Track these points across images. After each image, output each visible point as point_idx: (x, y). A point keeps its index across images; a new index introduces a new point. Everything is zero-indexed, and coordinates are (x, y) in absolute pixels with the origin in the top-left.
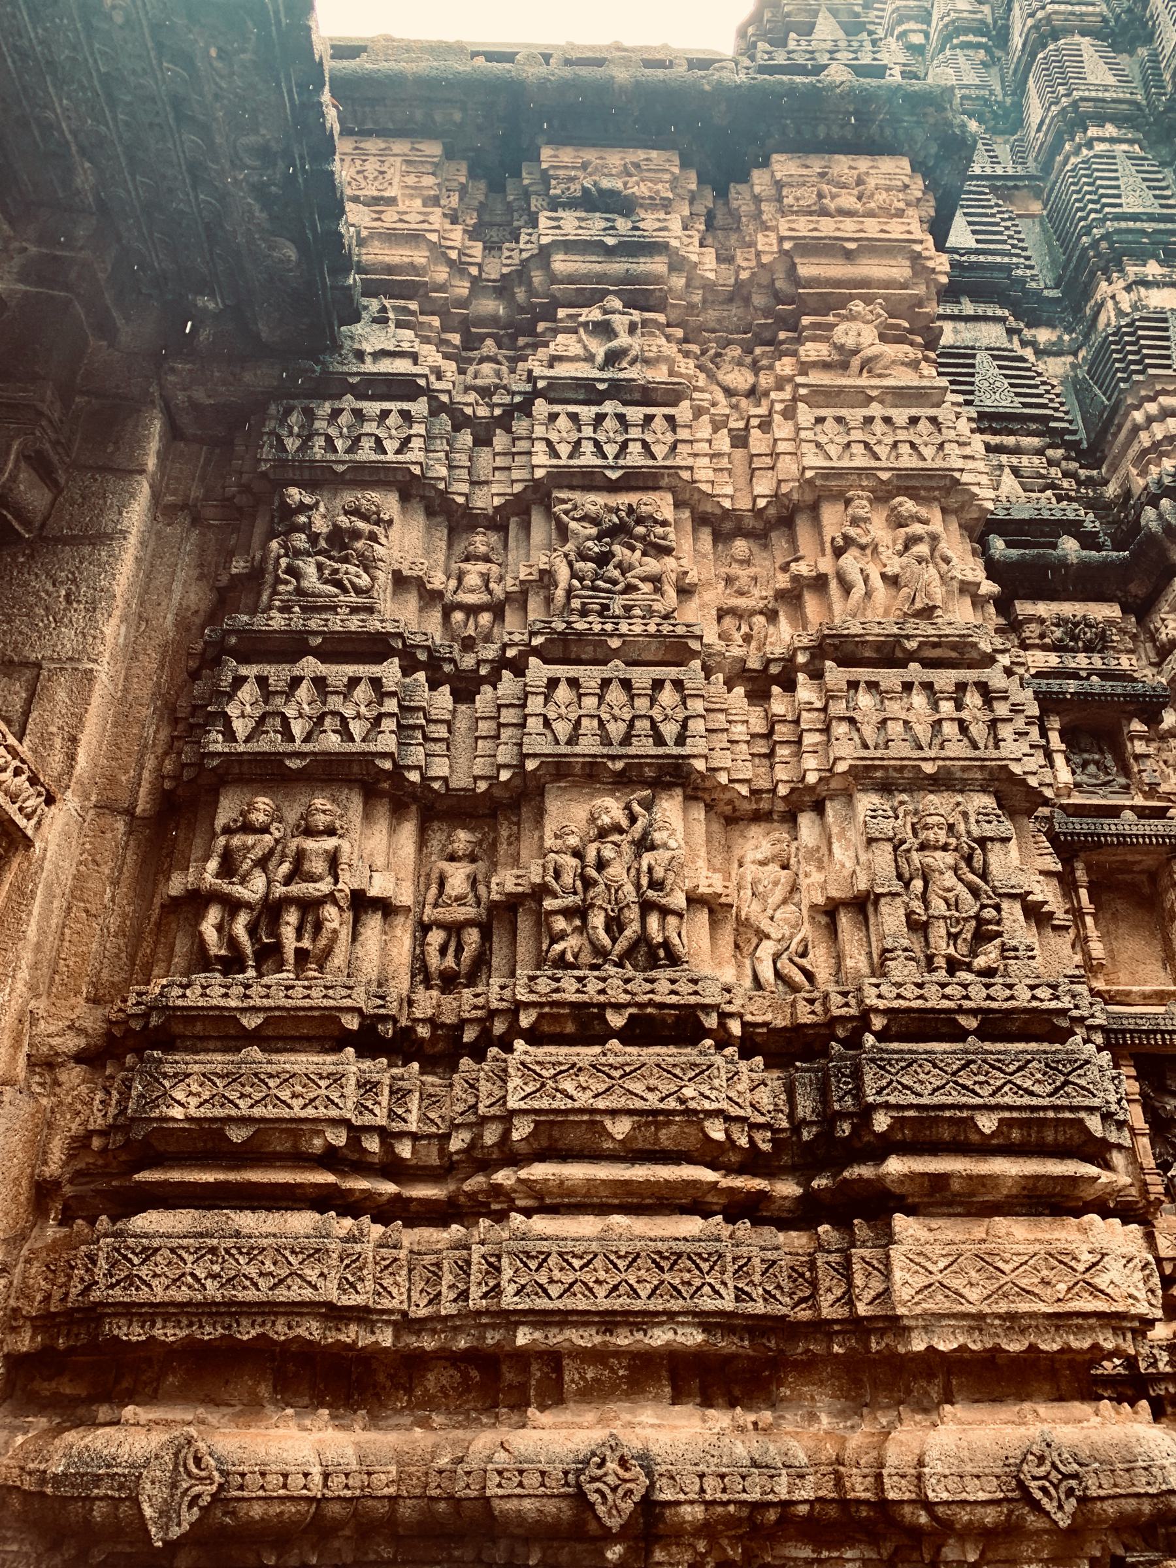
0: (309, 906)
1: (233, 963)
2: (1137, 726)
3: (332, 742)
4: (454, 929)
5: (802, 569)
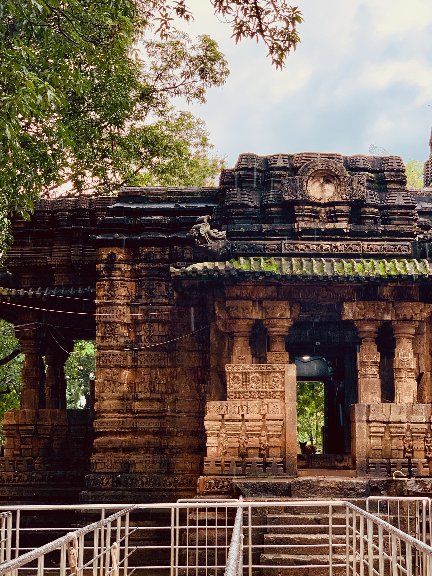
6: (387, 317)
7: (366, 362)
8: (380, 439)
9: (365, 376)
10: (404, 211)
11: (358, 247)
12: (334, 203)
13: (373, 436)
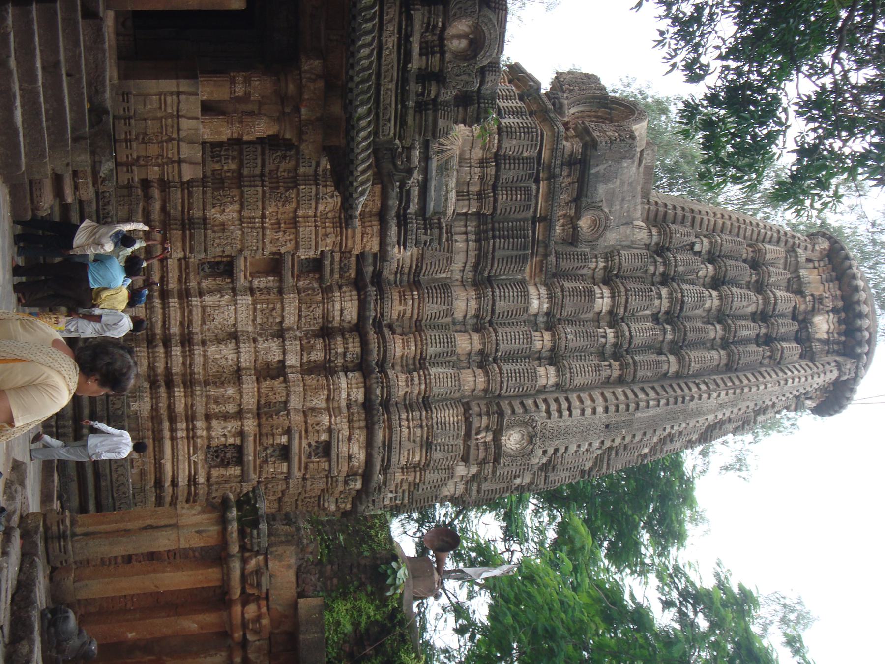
0: (220, 161)
1: (212, 152)
2: (317, 276)
3: (245, 162)
4: (221, 174)
5: (283, 225)
6: (303, 111)
7: (250, 85)
8: (158, 106)
9: (233, 82)
10: (430, 128)
11: (389, 79)
12: (443, 53)
13: (160, 99)
